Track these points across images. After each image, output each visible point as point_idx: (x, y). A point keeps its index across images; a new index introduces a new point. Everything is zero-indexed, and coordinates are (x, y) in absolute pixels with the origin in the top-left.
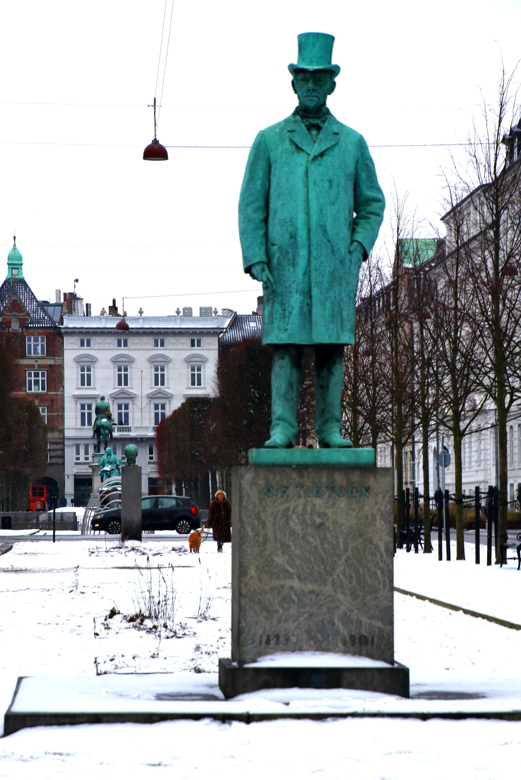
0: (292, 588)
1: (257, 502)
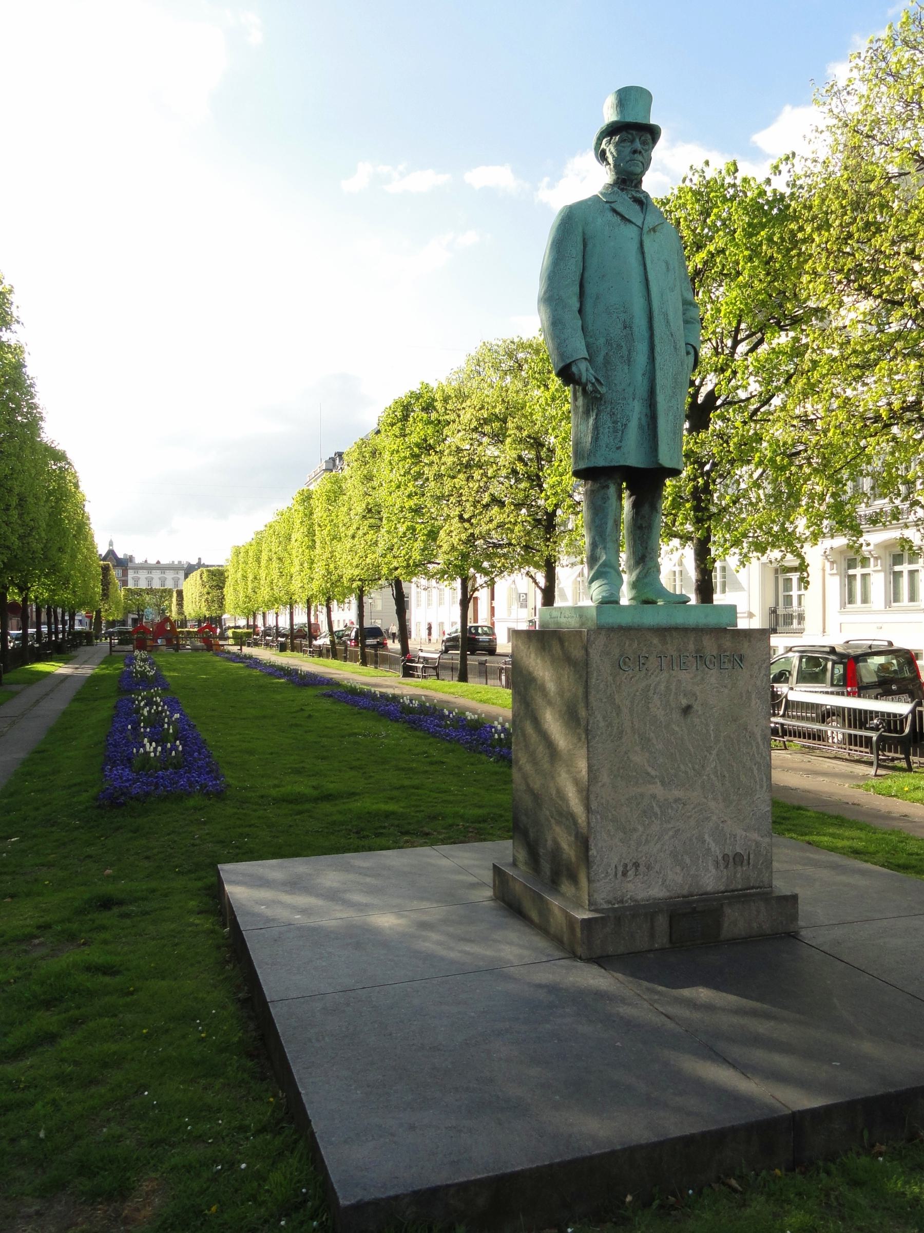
0: (654, 797)
1: (610, 678)
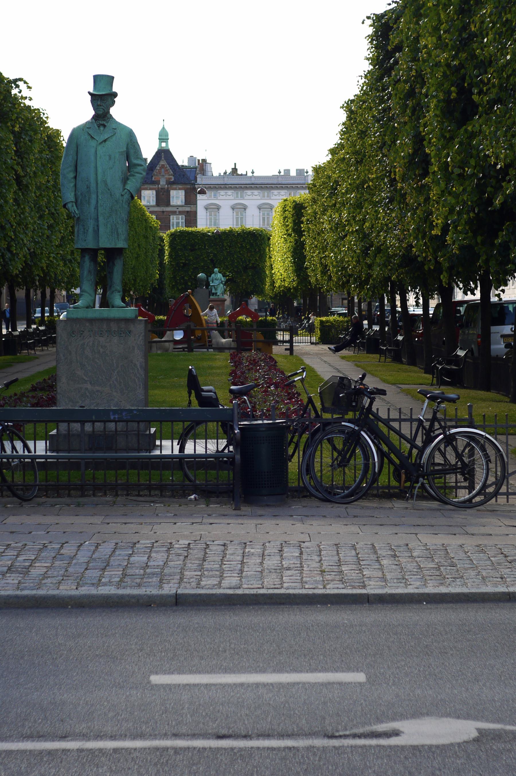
0: (87, 389)
1: (66, 340)
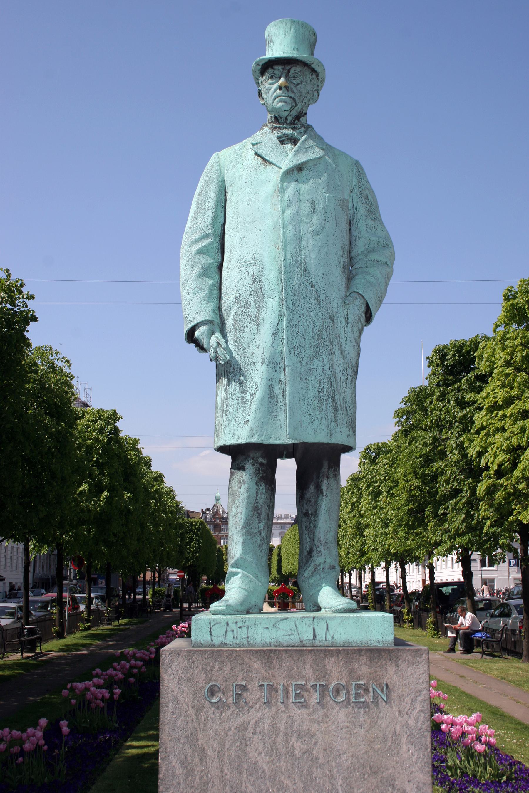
1: (191, 712)
